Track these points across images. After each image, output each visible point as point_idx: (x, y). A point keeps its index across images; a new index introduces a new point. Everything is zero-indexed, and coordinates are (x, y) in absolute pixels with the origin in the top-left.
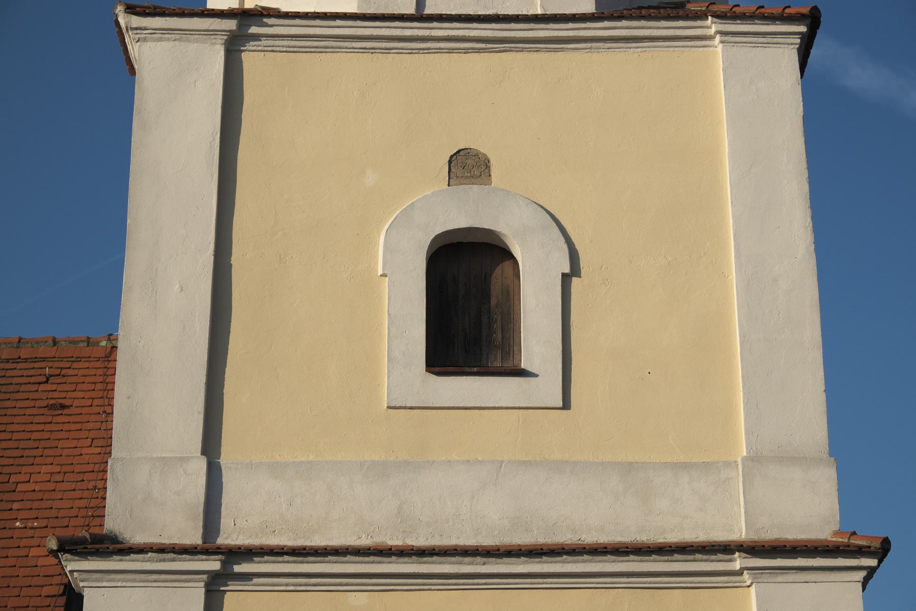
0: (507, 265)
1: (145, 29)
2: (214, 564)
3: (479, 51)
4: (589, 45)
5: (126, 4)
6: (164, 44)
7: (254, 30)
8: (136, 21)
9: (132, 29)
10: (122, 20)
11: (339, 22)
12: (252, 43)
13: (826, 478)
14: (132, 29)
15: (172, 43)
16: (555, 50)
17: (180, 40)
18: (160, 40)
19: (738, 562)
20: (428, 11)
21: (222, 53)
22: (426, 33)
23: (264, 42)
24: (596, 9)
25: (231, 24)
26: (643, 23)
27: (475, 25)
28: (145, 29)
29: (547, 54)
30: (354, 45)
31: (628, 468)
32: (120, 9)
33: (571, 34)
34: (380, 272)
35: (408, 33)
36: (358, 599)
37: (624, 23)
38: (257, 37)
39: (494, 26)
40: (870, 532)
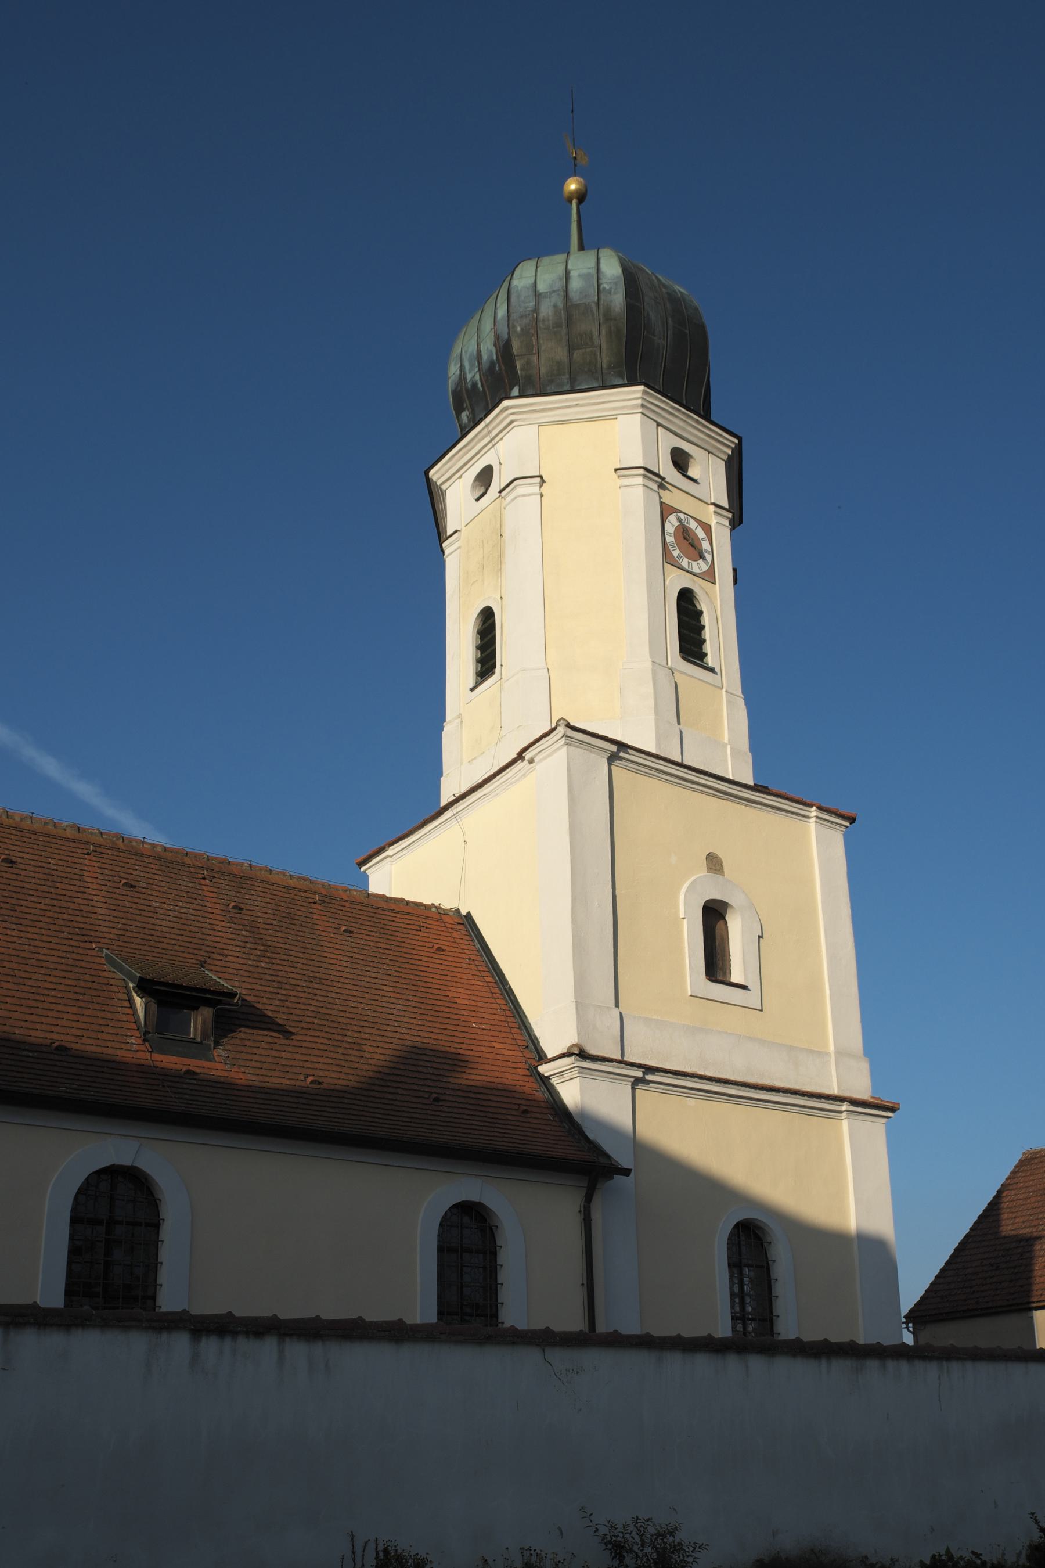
0: (722, 922)
2: (639, 1074)
7: (622, 754)
11: (661, 762)
13: (864, 1066)
19: (845, 1107)
22: (697, 779)
23: (624, 762)
25: (614, 748)
31: (791, 1048)
34: (682, 915)
36: (691, 1102)
40: (887, 1098)
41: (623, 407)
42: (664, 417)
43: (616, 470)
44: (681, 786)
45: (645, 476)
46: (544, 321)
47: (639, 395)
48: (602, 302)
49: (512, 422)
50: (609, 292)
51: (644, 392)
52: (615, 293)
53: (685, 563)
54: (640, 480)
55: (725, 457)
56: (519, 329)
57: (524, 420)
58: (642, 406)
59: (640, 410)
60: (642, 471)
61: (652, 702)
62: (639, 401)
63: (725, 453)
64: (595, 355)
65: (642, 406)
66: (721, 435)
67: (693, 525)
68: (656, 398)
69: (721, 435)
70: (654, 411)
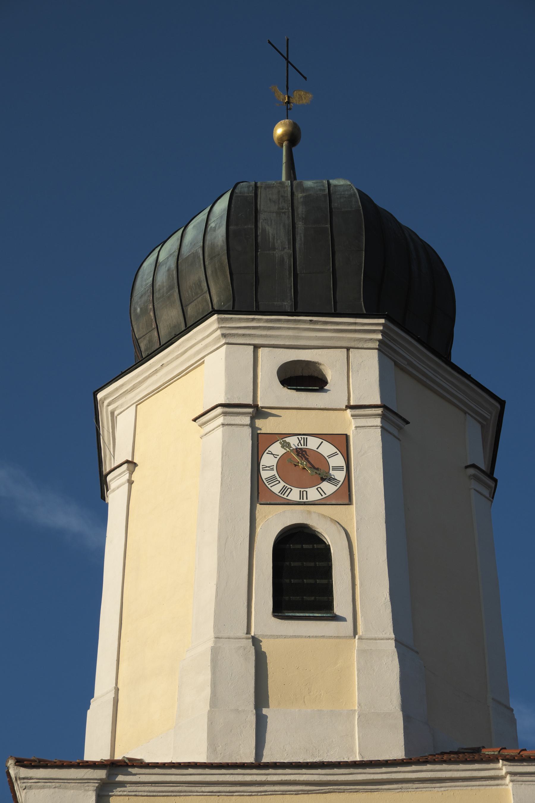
1: (31, 779)
3: (308, 792)
4: (400, 786)
5: (16, 759)
6: (46, 791)
7: (120, 778)
8: (24, 772)
9: (20, 779)
10: (12, 772)
11: (191, 771)
12: (119, 789)
14: (20, 779)
15: (52, 790)
16: (372, 791)
17: (59, 787)
18: (43, 787)
20: (266, 759)
21: (94, 798)
22: (263, 778)
23: (129, 788)
24: (406, 755)
25: (102, 774)
26: (445, 766)
27: (304, 771)
28: (31, 779)
29: (365, 794)
30: (203, 789)
32: (11, 763)
33: (385, 776)
35: (248, 778)
37: (429, 767)
38: (122, 784)
39: (319, 771)
41: (206, 346)
42: (266, 336)
43: (195, 420)
44: (241, 794)
45: (225, 414)
46: (159, 290)
47: (216, 326)
48: (207, 243)
49: (112, 413)
50: (214, 229)
51: (220, 320)
52: (219, 227)
53: (294, 495)
54: (221, 420)
55: (376, 345)
56: (139, 310)
57: (122, 405)
58: (224, 335)
59: (224, 342)
60: (219, 410)
61: (208, 691)
62: (219, 333)
63: (377, 340)
64: (206, 301)
65: (224, 335)
66: (355, 324)
67: (313, 443)
68: (240, 320)
69: (355, 324)
70: (244, 335)
